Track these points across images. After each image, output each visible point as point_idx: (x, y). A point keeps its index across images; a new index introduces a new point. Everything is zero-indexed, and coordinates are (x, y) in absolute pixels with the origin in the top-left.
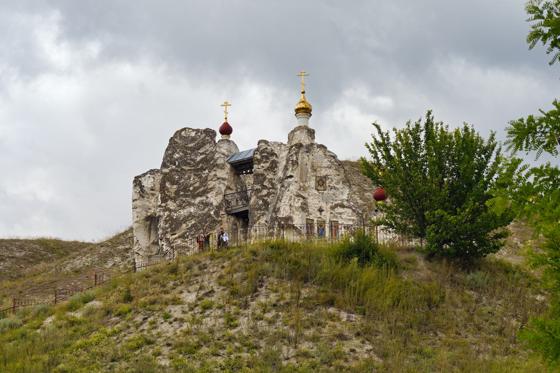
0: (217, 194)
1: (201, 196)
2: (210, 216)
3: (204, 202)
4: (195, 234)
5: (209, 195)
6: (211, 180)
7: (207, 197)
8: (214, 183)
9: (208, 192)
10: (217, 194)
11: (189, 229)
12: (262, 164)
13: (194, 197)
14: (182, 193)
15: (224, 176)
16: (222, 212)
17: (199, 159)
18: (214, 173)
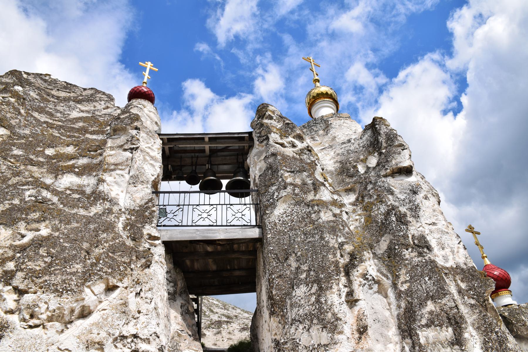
0: (135, 180)
1: (79, 174)
2: (110, 227)
3: (88, 190)
4: (47, 270)
5: (107, 177)
6: (121, 146)
7: (101, 181)
8: (128, 154)
9: (105, 171)
10: (135, 180)
11: (23, 249)
12: (290, 139)
13: (57, 171)
14: (17, 152)
15: (152, 154)
16: (149, 230)
17: (75, 114)
18: (134, 132)
